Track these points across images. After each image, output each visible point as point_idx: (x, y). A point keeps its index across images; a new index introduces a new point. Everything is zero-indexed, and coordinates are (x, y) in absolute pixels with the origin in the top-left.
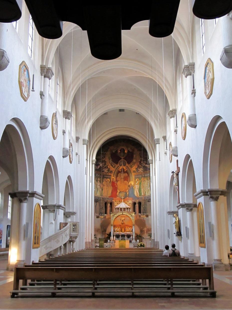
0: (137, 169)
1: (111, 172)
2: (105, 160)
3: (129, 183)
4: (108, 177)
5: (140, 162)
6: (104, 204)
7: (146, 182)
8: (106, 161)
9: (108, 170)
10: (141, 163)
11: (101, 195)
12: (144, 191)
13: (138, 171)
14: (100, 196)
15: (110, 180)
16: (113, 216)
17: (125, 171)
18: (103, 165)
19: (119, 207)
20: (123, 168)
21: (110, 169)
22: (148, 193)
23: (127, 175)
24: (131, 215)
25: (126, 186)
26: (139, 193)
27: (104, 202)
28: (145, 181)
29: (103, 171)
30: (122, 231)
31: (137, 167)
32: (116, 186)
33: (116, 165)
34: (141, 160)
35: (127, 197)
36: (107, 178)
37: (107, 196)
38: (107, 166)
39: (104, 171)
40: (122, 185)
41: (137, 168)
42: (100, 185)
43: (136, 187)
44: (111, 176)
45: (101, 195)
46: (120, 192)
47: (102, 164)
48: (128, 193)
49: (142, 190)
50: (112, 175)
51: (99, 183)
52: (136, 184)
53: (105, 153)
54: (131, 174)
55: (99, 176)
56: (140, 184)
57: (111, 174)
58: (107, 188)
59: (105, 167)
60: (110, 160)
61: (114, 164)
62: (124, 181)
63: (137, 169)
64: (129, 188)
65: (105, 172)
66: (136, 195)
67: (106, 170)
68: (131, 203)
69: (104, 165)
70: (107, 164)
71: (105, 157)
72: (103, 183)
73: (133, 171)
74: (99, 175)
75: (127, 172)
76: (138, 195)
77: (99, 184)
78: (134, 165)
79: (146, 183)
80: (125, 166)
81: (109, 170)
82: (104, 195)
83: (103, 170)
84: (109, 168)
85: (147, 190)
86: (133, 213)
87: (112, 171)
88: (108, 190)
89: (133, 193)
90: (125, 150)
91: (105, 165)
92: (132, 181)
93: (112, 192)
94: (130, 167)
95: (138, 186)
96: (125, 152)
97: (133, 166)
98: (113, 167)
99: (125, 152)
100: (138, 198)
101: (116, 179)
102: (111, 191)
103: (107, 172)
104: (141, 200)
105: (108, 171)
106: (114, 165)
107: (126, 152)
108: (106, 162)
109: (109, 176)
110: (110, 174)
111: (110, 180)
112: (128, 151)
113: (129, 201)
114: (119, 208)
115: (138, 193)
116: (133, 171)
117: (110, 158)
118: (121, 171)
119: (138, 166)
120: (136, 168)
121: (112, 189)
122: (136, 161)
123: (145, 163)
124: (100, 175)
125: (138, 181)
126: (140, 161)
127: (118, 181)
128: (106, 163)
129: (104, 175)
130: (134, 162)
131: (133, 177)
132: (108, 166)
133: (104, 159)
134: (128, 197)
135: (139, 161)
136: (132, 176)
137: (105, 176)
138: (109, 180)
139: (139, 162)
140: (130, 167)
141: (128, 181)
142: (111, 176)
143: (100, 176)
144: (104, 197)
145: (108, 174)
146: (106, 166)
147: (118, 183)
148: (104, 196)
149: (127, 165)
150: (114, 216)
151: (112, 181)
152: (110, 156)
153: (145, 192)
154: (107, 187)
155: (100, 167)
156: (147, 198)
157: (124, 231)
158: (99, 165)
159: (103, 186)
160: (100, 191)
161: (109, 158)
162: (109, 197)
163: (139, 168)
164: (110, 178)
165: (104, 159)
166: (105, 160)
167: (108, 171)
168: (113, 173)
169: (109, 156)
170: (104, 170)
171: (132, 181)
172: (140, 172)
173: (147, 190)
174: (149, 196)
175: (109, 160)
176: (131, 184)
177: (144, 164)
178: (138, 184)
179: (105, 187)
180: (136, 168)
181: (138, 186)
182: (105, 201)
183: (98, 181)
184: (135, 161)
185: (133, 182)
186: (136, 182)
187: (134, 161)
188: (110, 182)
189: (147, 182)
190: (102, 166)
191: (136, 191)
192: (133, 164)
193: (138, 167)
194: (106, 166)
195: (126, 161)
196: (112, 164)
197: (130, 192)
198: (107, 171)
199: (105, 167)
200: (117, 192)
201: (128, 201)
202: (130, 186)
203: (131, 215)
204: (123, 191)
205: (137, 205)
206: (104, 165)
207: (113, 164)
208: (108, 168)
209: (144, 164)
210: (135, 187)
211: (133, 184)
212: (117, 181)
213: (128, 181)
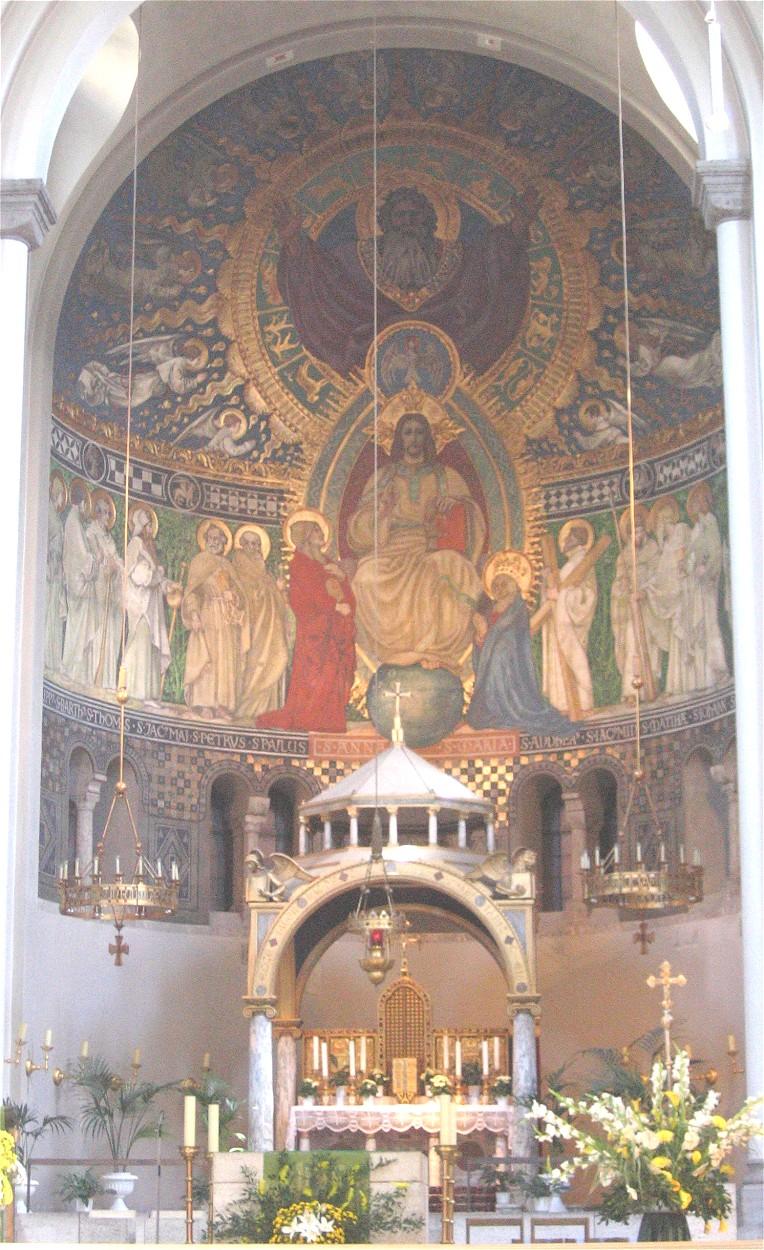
0: (566, 419)
1: (282, 460)
2: (214, 323)
3: (480, 572)
4: (253, 504)
5: (604, 336)
6: (207, 792)
7: (673, 547)
8: (227, 329)
9: (251, 434)
10: (610, 345)
11: (167, 697)
12: (646, 641)
13: (577, 435)
14: (154, 707)
15: (277, 546)
16: (276, 896)
17: (439, 449)
18: (189, 374)
19: (349, 801)
20: (421, 419)
21: (275, 419)
22: (691, 660)
23: (465, 490)
24: (490, 884)
25: (447, 605)
26: (593, 677)
27: (201, 770)
28: (660, 534)
29: (197, 443)
31: (561, 401)
32: (343, 609)
33: (338, 381)
34: (611, 319)
35: (466, 729)
36: (244, 517)
37: (232, 714)
38: (240, 391)
39: (207, 440)
40: (406, 598)
41: (572, 409)
42: (153, 588)
43: (562, 616)
44: (280, 494)
45: (167, 697)
46: (385, 669)
47: (179, 361)
48: (468, 685)
49: (628, 638)
50: (299, 489)
51: (141, 558)
52: (559, 586)
53: (214, 234)
54: (510, 474)
55: (147, 487)
56: (603, 572)
57: (283, 474)
58: (239, 628)
59: (221, 402)
60: (274, 329)
61: (317, 377)
62: (430, 551)
63: (566, 419)
64: (482, 627)
65: (220, 454)
66: (559, 698)
67: (228, 435)
68: (502, 793)
69: (200, 378)
70: (238, 365)
71: (213, 288)
72: (198, 566)
73: (520, 447)
74: (147, 476)
75: (455, 457)
76: (585, 698)
77: (143, 573)
78: (537, 377)
79: (670, 555)
80: (437, 392)
81: (268, 431)
82: (196, 702)
83: (199, 432)
84: (266, 417)
85: (680, 633)
86: (520, 865)
87: (297, 446)
88: (246, 646)
89: (529, 681)
90: (440, 213)
91: (223, 371)
92: (517, 542)
93: (291, 673)
94: (489, 407)
95: (584, 601)
96: (439, 234)
97: (523, 384)
98: (313, 408)
99: (439, 234)
100: (583, 733)
101: (342, 528)
102: (281, 661)
103: (242, 457)
104: (614, 753)
105: (248, 445)
106: (318, 386)
107: (446, 231)
108: (229, 343)
109: (263, 493)
110: (270, 480)
111: (277, 546)
112: (471, 218)
113: (487, 770)
114: (352, 811)
115: (583, 674)
116: (529, 442)
117: (276, 300)
118: (398, 445)
119: (579, 378)
120: (559, 412)
121: (292, 638)
122: (555, 327)
123: (653, 342)
124: (156, 480)
125: (583, 542)
126: (606, 326)
127: (368, 550)
128: (223, 355)
129: (201, 486)
130: (534, 343)
131: (533, 507)
132: (254, 396)
133: (205, 312)
134: (468, 720)
135: (593, 324)
136: (515, 501)
137: (215, 498)
138: (258, 543)
139: (594, 335)
140: (489, 407)
141: (466, 553)
142: (280, 494)
143: (157, 490)
144: (206, 719)
145: (248, 478)
146: (228, 386)
147: (368, 574)
148: (198, 710)
149: (460, 380)
150: (284, 898)
151: (292, 547)
152: (270, 273)
153: (664, 656)
154: (240, 618)
155: (166, 392)
156: (680, 724)
157: (413, 1087)
158: (150, 367)
159: (191, 601)
160: (155, 651)
161: (261, 301)
162: (265, 721)
163: (593, 411)
164: (274, 525)
165: (205, 312)
166: (214, 323)
167: (248, 445)
168: (307, 472)
169: (260, 277)
170: (201, 427)
171: (517, 542)
172: (606, 444)
173: (680, 633)
174: (699, 694)
175: (265, 321)
176: (501, 583)
177: (644, 351)
178: (576, 581)
179: (217, 613)
180: (559, 412)
181: (584, 601)
182: (208, 763)
183: (136, 546)
184: (547, 332)
185: (524, 563)
186: (562, 561)
187: (539, 327)
188: (272, 562)
189: (687, 538)
190: (177, 383)
191: (561, 653)
192: (523, 373)
193: (581, 395)
194: (228, 386)
195: (446, 339)
196: (294, 368)
197: (496, 669)
198: (239, 442)
199: (221, 402)
200: (350, 665)
201: (471, 763)
202: (501, 607)
203: (490, 884)
204: (417, 665)
205: (574, 811)
206: (200, 378)
207: (304, 371)
208: (248, 411)
209: (644, 351)
210: (549, 616)
211: (525, 582)
212: (350, 552)
213: (476, 556)
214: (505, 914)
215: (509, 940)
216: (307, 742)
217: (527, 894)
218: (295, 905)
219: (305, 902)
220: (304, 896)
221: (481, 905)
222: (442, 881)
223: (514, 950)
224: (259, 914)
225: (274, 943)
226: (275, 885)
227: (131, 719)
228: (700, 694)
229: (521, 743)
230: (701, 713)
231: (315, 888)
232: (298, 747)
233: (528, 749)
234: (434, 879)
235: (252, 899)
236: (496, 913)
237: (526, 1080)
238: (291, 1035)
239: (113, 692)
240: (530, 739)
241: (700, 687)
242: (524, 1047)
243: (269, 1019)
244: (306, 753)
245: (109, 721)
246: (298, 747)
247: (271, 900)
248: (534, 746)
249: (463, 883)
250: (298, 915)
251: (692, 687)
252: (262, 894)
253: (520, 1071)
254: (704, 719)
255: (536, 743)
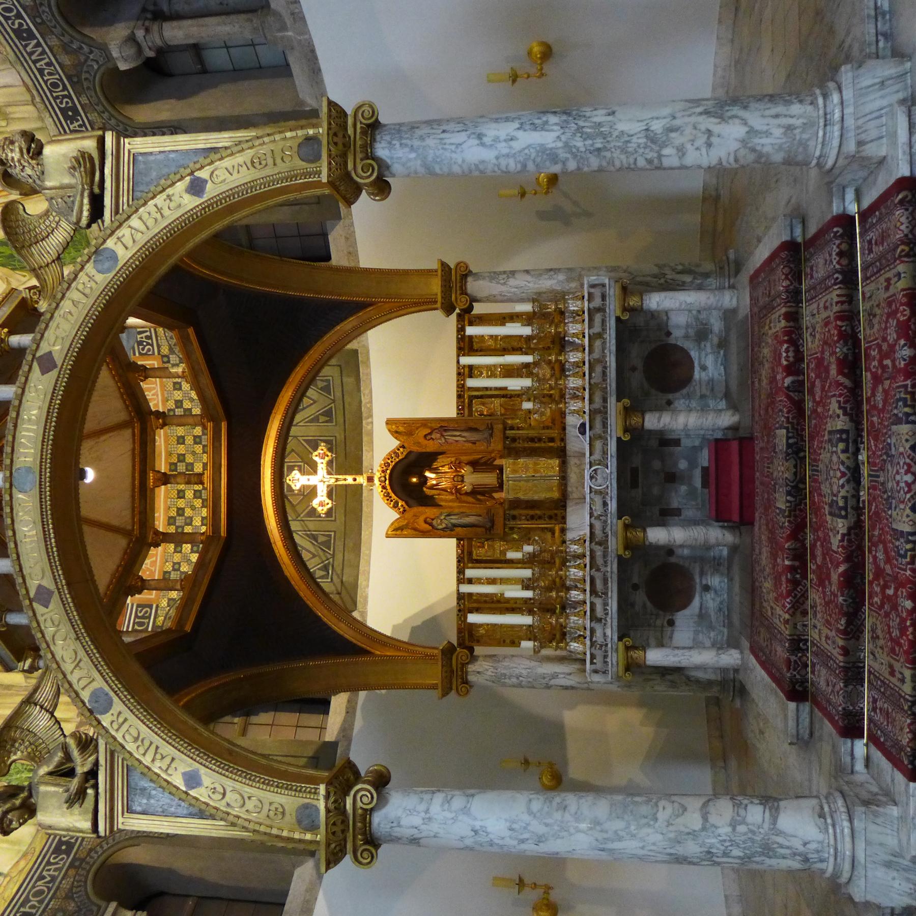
30: (556, 495)
214: (139, 200)
215: (197, 187)
216: (138, 606)
217: (89, 145)
218: (106, 720)
219: (95, 695)
220: (85, 695)
221: (114, 257)
222: (58, 359)
223: (222, 175)
224: (130, 810)
225: (192, 780)
226: (61, 764)
227: (53, 853)
228: (35, 92)
229: (146, 354)
230: (59, 92)
231: (68, 667)
232: (143, 617)
233: (152, 345)
234: (54, 374)
235: (87, 825)
236: (135, 222)
237: (544, 127)
238: (464, 665)
239: (8, 879)
240: (140, 343)
241: (28, 97)
242: (461, 137)
243: (382, 800)
244: (151, 607)
245: (41, 892)
246: (143, 617)
247: (92, 774)
248: (147, 337)
249: (66, 305)
250: (127, 714)
251: (31, 108)
252: (79, 797)
253: (517, 145)
254: (65, 88)
255: (144, 335)
